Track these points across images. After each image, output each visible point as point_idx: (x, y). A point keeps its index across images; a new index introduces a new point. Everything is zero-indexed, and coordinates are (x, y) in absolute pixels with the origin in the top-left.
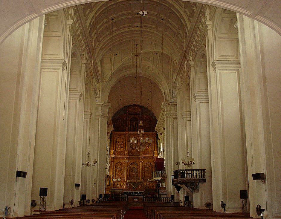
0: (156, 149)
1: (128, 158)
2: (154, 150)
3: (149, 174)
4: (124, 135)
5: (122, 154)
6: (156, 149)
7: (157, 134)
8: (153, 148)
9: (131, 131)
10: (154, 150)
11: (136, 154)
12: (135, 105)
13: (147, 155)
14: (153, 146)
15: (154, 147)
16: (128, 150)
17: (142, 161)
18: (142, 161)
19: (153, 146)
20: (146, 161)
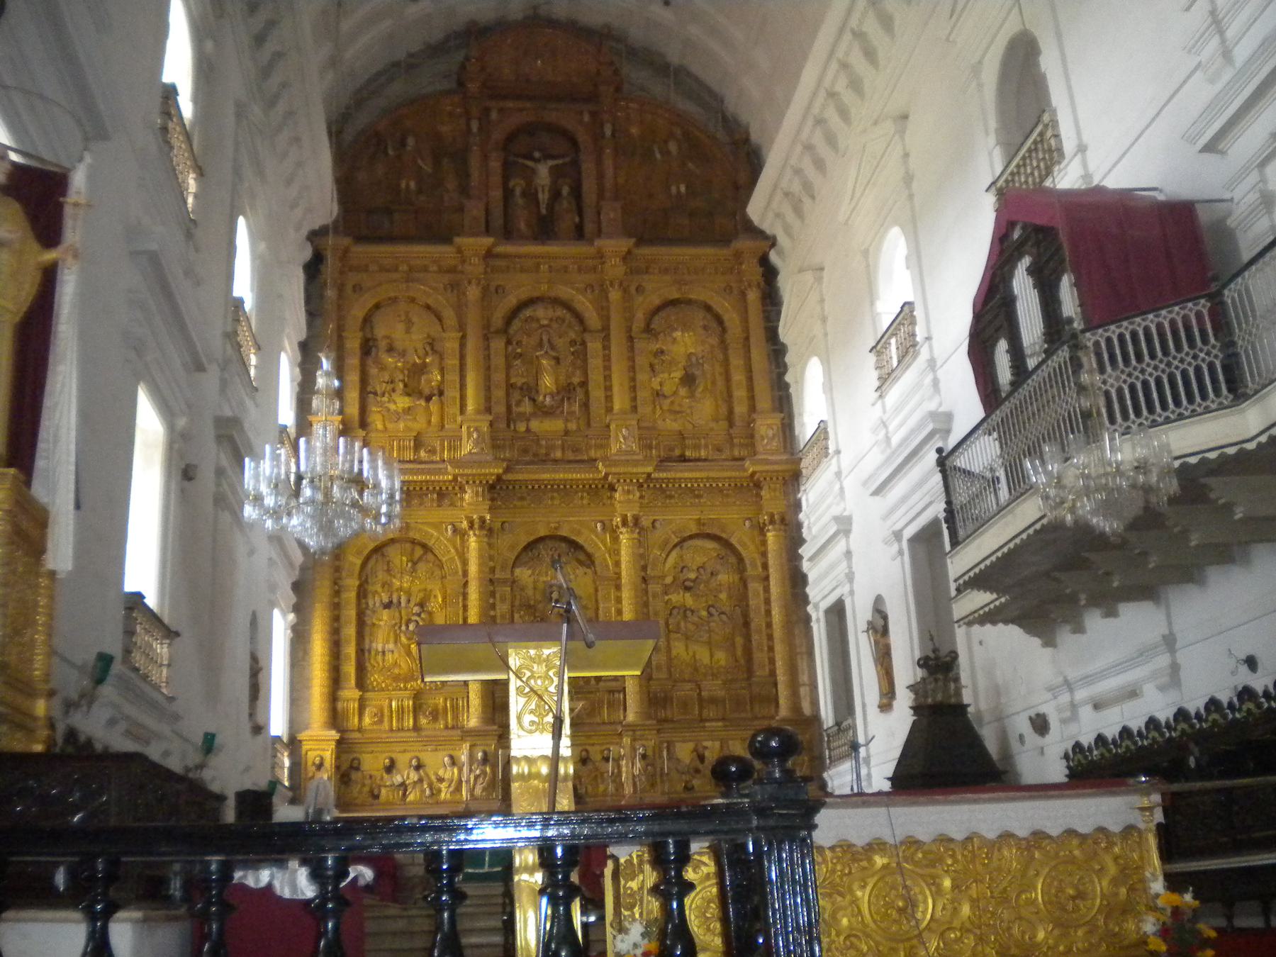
0: (764, 402)
1: (496, 489)
2: (753, 408)
3: (709, 643)
4: (446, 278)
5: (432, 451)
6: (764, 402)
7: (764, 261)
8: (740, 393)
9: (508, 233)
10: (753, 408)
11: (576, 450)
12: (536, 22)
13: (683, 459)
14: (738, 377)
15: (751, 388)
16: (488, 410)
17: (636, 520)
18: (636, 520)
19: (738, 377)
20: (683, 518)
